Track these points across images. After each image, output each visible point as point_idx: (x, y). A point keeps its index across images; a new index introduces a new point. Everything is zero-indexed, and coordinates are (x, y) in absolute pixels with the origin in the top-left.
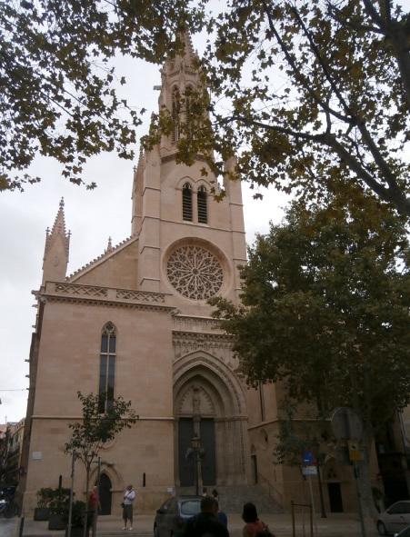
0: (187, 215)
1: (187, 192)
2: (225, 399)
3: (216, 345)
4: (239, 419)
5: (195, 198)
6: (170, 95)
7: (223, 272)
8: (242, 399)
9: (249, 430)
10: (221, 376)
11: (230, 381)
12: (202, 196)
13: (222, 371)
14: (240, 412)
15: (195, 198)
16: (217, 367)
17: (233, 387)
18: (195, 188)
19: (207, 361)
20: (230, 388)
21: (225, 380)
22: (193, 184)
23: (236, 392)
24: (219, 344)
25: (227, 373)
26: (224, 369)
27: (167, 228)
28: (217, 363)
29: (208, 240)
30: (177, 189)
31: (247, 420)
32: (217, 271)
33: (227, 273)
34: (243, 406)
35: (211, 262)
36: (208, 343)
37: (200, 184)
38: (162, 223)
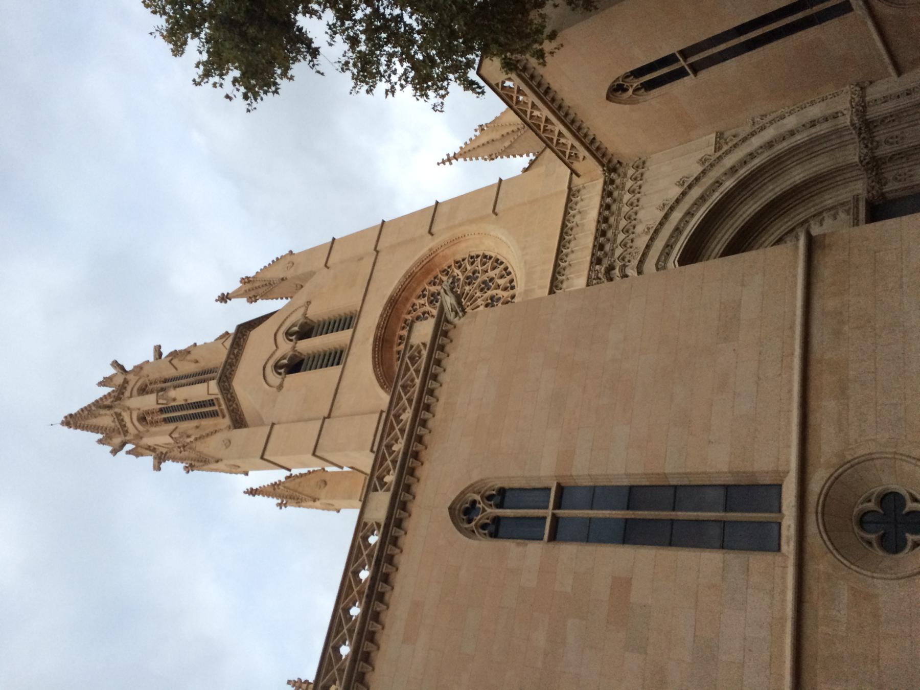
0: (335, 357)
1: (295, 365)
2: (797, 175)
3: (626, 231)
4: (861, 108)
5: (307, 346)
6: (153, 429)
7: (459, 258)
8: (791, 122)
9: (899, 73)
10: (716, 197)
11: (733, 170)
12: (306, 331)
13: (703, 198)
14: (835, 116)
15: (307, 346)
16: (689, 214)
17: (752, 156)
18: (286, 347)
19: (669, 246)
20: (757, 162)
21: (729, 184)
22: (278, 355)
23: (770, 145)
24: (623, 223)
25: (707, 181)
26: (696, 193)
27: (346, 401)
28: (677, 215)
29: (385, 301)
30: (280, 387)
31: (863, 89)
32: (457, 272)
33: (463, 245)
34: (815, 111)
35: (433, 289)
36: (619, 251)
37: (281, 337)
38: (332, 415)
